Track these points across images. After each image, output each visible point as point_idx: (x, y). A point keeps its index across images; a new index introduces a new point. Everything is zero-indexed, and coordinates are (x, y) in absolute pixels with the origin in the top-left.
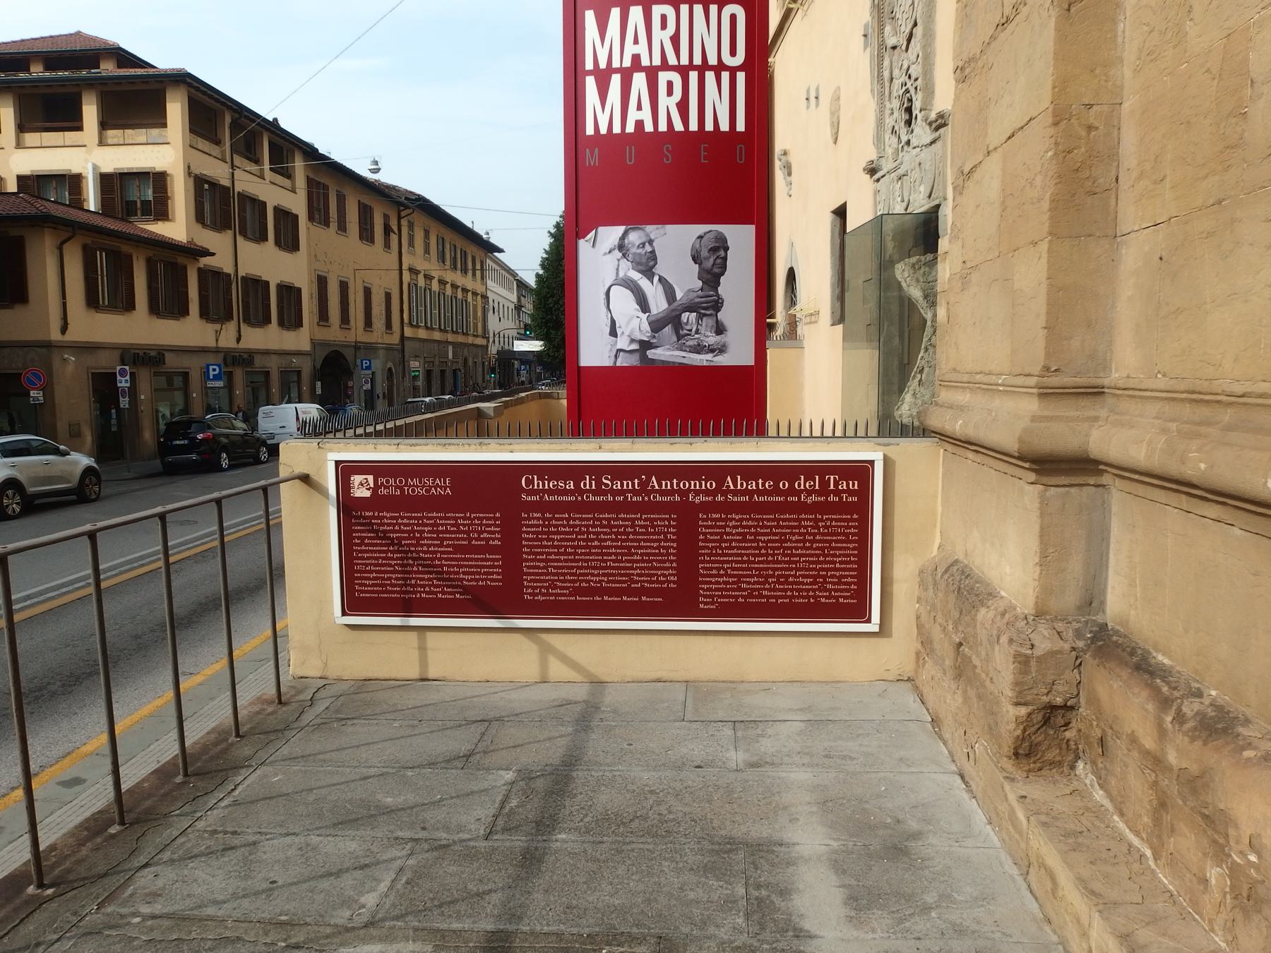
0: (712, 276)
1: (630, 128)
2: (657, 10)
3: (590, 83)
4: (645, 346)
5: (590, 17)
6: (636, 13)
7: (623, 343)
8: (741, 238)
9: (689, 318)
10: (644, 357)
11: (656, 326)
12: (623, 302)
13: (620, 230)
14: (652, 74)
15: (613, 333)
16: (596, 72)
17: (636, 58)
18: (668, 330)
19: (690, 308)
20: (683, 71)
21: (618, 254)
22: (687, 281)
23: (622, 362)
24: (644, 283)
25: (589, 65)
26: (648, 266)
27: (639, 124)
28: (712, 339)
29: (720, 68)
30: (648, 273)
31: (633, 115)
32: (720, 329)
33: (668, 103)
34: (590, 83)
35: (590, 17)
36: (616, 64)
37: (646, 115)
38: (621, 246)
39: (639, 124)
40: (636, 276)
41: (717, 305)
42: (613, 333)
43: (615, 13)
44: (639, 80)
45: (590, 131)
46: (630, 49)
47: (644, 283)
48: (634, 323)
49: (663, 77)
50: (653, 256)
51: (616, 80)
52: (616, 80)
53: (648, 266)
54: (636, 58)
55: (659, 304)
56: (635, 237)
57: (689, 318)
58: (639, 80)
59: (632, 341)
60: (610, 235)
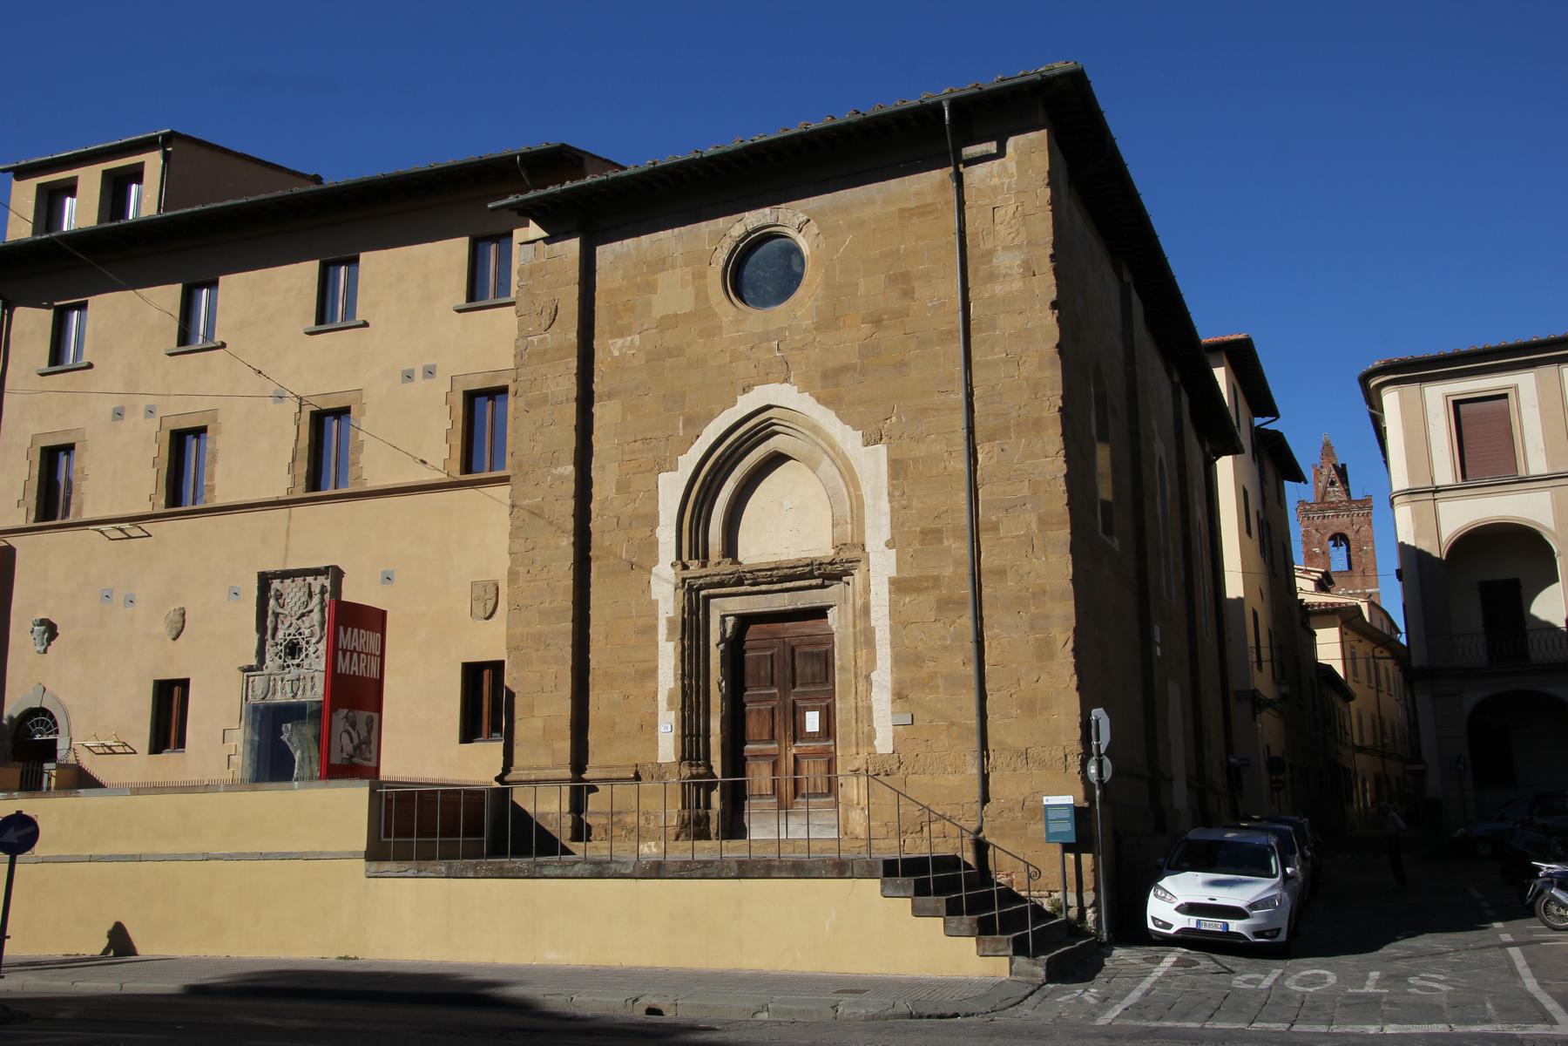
0: (369, 732)
1: (352, 673)
2: (362, 631)
3: (340, 652)
4: (351, 756)
5: (341, 628)
6: (356, 630)
7: (345, 755)
8: (375, 716)
9: (364, 746)
10: (351, 762)
11: (355, 748)
12: (345, 739)
13: (346, 711)
14: (359, 653)
15: (342, 751)
16: (342, 649)
17: (355, 647)
18: (358, 751)
19: (364, 743)
20: (367, 654)
21: (345, 720)
22: (364, 734)
23: (345, 762)
24: (352, 732)
25: (340, 647)
26: (353, 725)
27: (354, 671)
28: (369, 756)
29: (375, 655)
30: (354, 728)
31: (353, 669)
32: (370, 753)
33: (362, 665)
34: (340, 652)
35: (341, 628)
36: (349, 648)
37: (356, 669)
38: (346, 717)
39: (354, 671)
40: (350, 729)
41: (370, 742)
42: (342, 751)
43: (350, 629)
44: (355, 655)
45: (339, 671)
46: (353, 644)
47: (352, 732)
48: (348, 747)
49: (362, 656)
50: (355, 722)
51: (348, 653)
52: (348, 653)
53: (353, 725)
54: (355, 647)
55: (356, 741)
56: (350, 714)
57: (364, 746)
58: (355, 655)
59: (348, 755)
60: (343, 712)
